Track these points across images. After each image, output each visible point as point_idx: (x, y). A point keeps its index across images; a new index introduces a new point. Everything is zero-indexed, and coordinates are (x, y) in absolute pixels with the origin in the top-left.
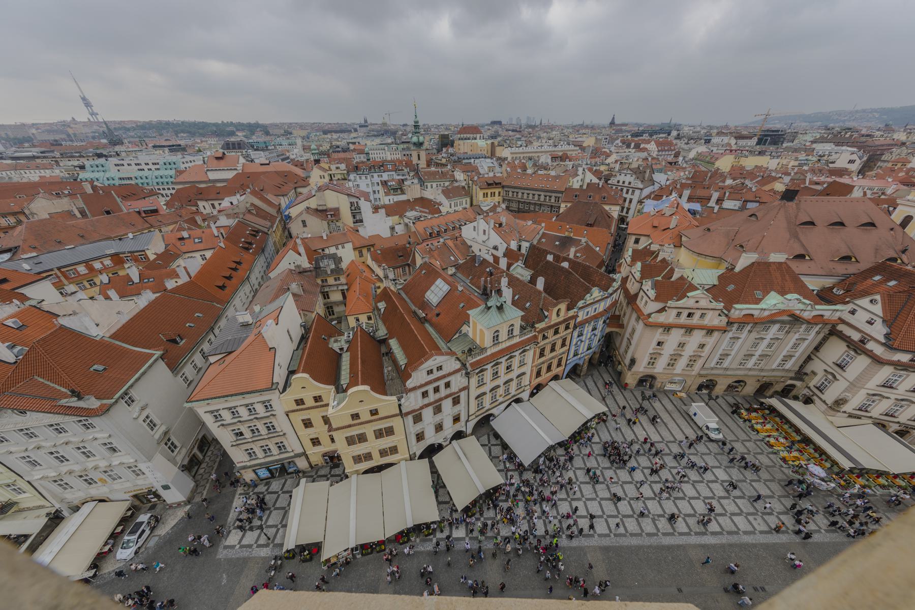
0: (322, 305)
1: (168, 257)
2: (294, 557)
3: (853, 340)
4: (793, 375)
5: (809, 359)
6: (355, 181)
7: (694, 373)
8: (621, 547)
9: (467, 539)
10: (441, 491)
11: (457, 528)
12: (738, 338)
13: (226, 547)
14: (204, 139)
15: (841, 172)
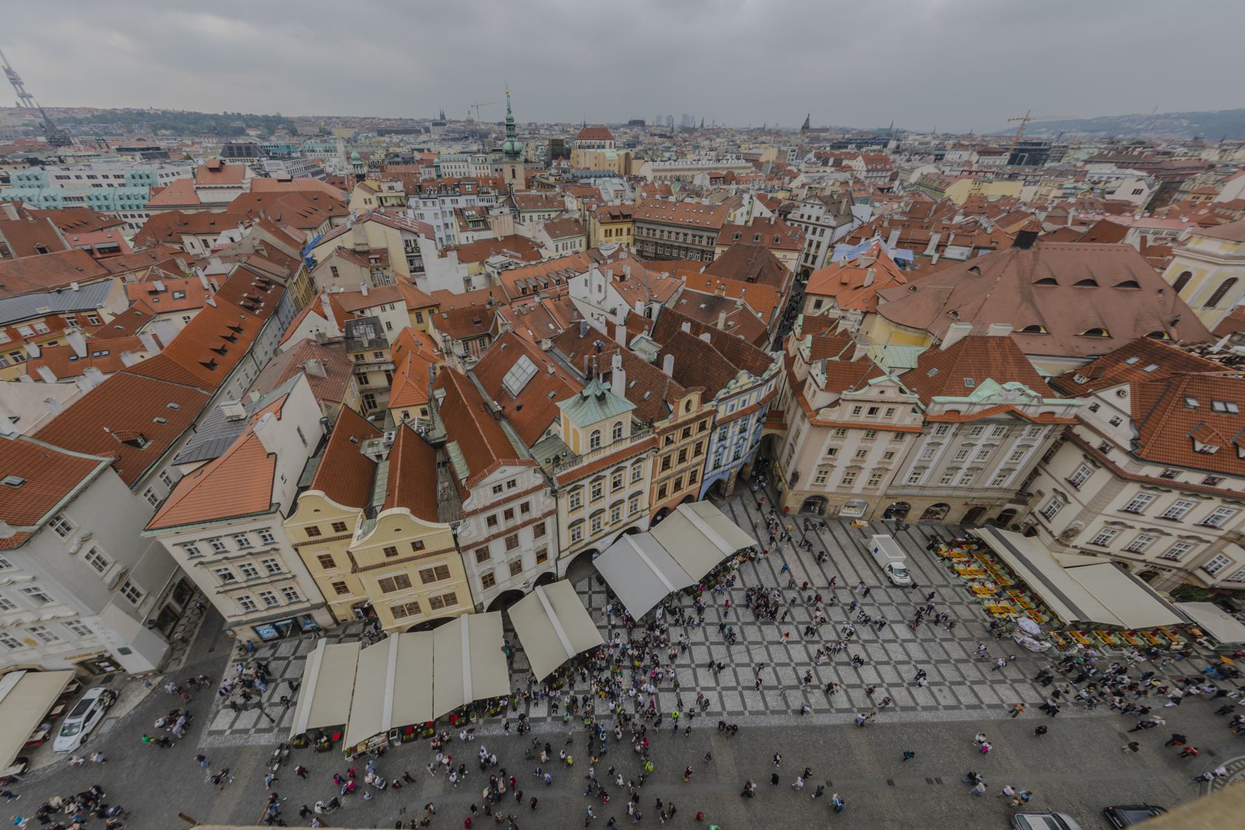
0: (357, 393)
1: (133, 319)
2: (306, 745)
3: (1091, 448)
4: (1012, 496)
5: (1035, 473)
6: (417, 207)
7: (878, 493)
8: (758, 729)
9: (549, 720)
10: (518, 656)
11: (536, 704)
12: (939, 444)
13: (211, 733)
14: (197, 140)
15: (1121, 208)
